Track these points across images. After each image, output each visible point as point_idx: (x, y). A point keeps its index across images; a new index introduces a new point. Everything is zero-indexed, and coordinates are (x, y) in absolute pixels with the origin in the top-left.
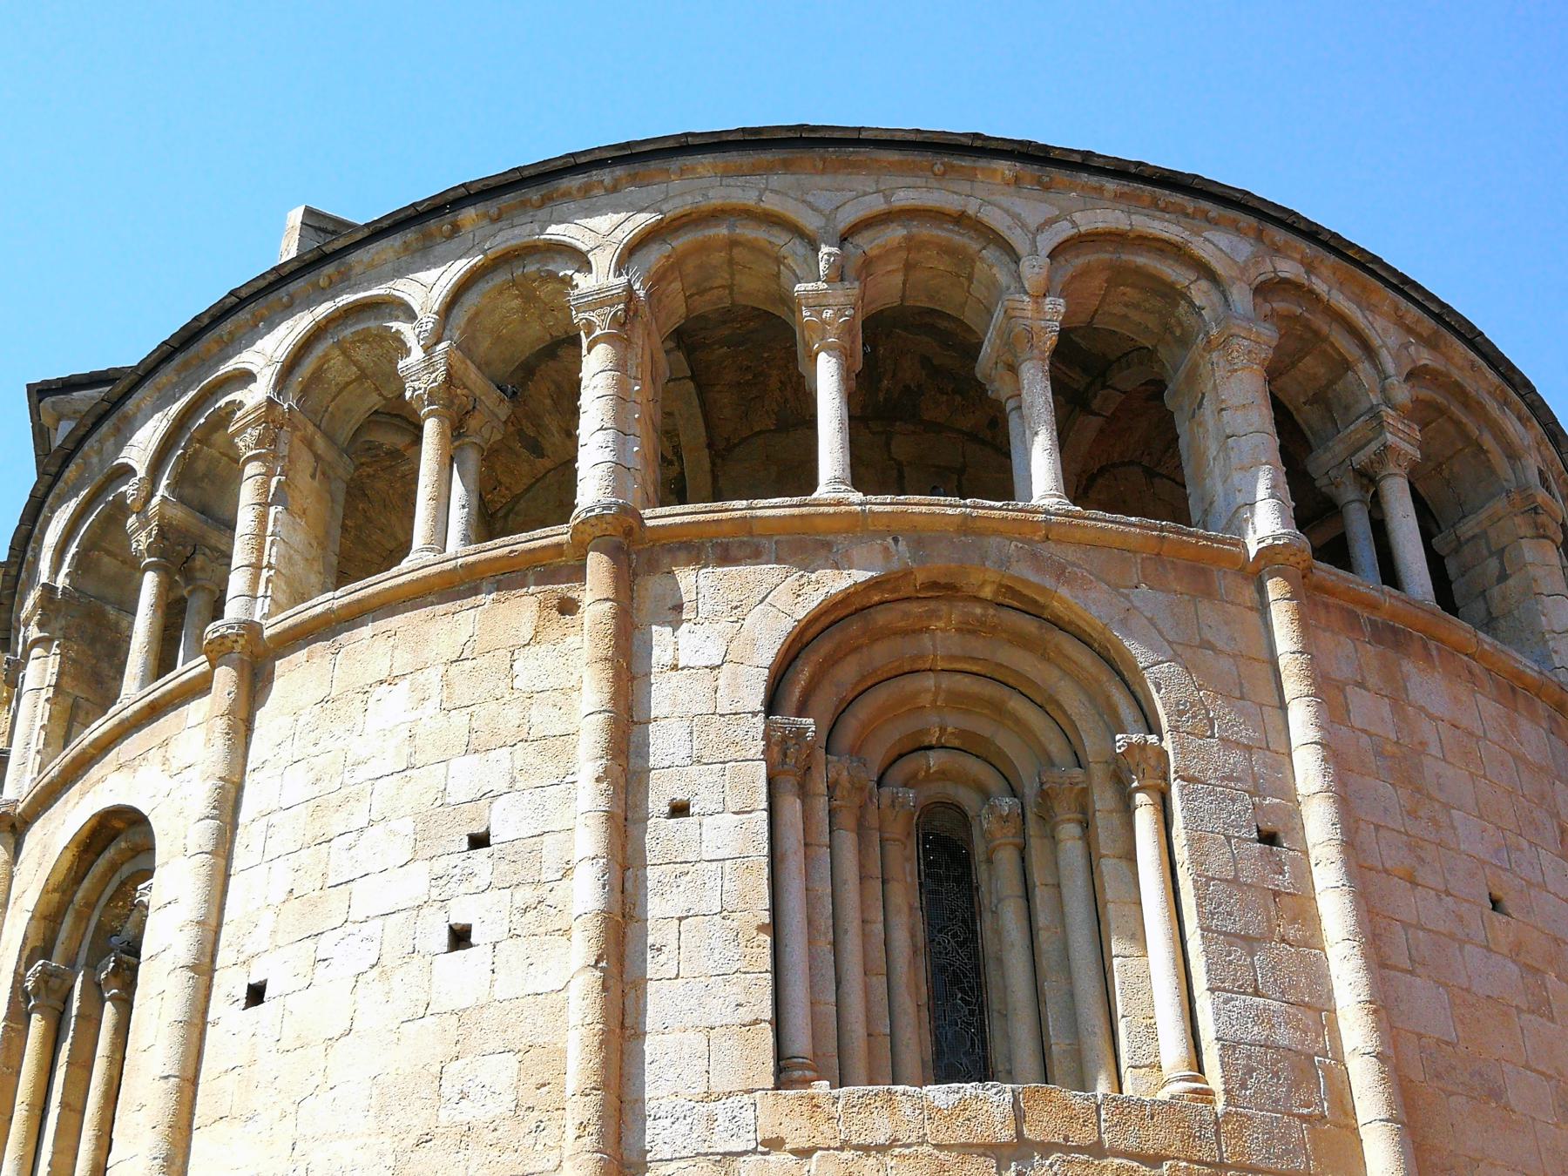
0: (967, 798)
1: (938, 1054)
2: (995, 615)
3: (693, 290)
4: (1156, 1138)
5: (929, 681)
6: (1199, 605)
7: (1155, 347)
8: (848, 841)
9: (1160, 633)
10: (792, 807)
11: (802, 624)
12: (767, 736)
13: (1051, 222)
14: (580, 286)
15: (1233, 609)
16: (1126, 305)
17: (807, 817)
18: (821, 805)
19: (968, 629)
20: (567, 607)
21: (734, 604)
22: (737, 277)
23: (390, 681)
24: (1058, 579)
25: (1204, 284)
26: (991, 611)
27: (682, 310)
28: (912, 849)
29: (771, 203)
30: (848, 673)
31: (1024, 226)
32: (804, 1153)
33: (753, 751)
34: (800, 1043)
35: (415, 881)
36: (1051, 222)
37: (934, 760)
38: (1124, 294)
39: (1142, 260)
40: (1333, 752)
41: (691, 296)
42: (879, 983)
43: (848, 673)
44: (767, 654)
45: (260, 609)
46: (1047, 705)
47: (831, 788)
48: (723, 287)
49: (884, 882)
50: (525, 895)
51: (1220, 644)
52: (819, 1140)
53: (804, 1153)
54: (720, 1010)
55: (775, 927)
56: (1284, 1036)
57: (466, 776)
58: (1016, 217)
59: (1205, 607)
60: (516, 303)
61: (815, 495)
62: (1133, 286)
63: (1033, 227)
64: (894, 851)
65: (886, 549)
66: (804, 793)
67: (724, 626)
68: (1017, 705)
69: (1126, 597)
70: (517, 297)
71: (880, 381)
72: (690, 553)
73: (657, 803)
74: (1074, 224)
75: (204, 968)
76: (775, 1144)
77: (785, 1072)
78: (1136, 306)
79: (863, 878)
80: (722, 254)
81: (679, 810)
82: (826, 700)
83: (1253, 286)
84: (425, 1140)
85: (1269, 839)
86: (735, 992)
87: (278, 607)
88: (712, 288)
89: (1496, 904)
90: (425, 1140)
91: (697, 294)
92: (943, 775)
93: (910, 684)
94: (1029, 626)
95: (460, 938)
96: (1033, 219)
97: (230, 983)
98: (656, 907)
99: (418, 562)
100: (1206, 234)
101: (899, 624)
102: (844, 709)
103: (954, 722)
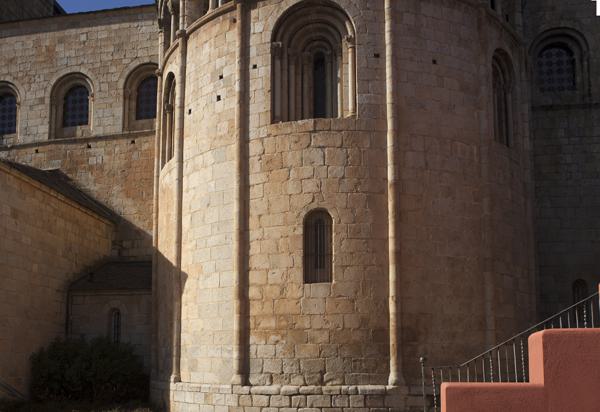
0: (324, 51)
1: (315, 111)
4: (342, 126)
5: (311, 26)
8: (292, 67)
10: (278, 63)
12: (271, 48)
17: (281, 65)
18: (285, 61)
19: (318, 12)
20: (235, 21)
23: (206, 42)
28: (312, 64)
30: (292, 28)
32: (275, 136)
34: (278, 113)
35: (210, 88)
37: (316, 43)
40: (393, 32)
42: (299, 98)
43: (292, 28)
44: (271, 28)
45: (186, 25)
46: (336, 28)
47: (288, 55)
49: (302, 74)
50: (229, 88)
53: (275, 136)
54: (262, 110)
55: (273, 91)
56: (373, 102)
57: (219, 62)
64: (305, 68)
66: (281, 58)
67: (263, 22)
68: (332, 30)
73: (251, 66)
75: (182, 107)
76: (269, 136)
77: (274, 120)
79: (296, 73)
81: (255, 67)
82: (287, 37)
84: (215, 139)
85: (377, 56)
86: (264, 105)
87: (189, 25)
89: (434, 62)
90: (215, 139)
92: (318, 46)
93: (308, 27)
94: (330, 10)
95: (219, 98)
97: (186, 110)
98: (252, 89)
99: (210, 12)
102: (293, 35)
103: (318, 34)
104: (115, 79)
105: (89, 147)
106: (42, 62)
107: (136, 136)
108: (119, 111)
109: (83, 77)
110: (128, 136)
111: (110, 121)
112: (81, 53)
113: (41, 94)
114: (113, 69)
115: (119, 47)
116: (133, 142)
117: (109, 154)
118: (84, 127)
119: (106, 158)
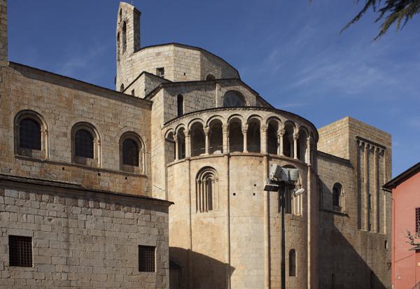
104: (114, 136)
105: (99, 174)
106: (61, 107)
107: (129, 175)
108: (117, 157)
109: (92, 127)
110: (123, 174)
111: (112, 161)
112: (92, 111)
113: (64, 130)
114: (112, 129)
115: (116, 116)
116: (126, 178)
117: (113, 182)
118: (91, 159)
119: (111, 184)
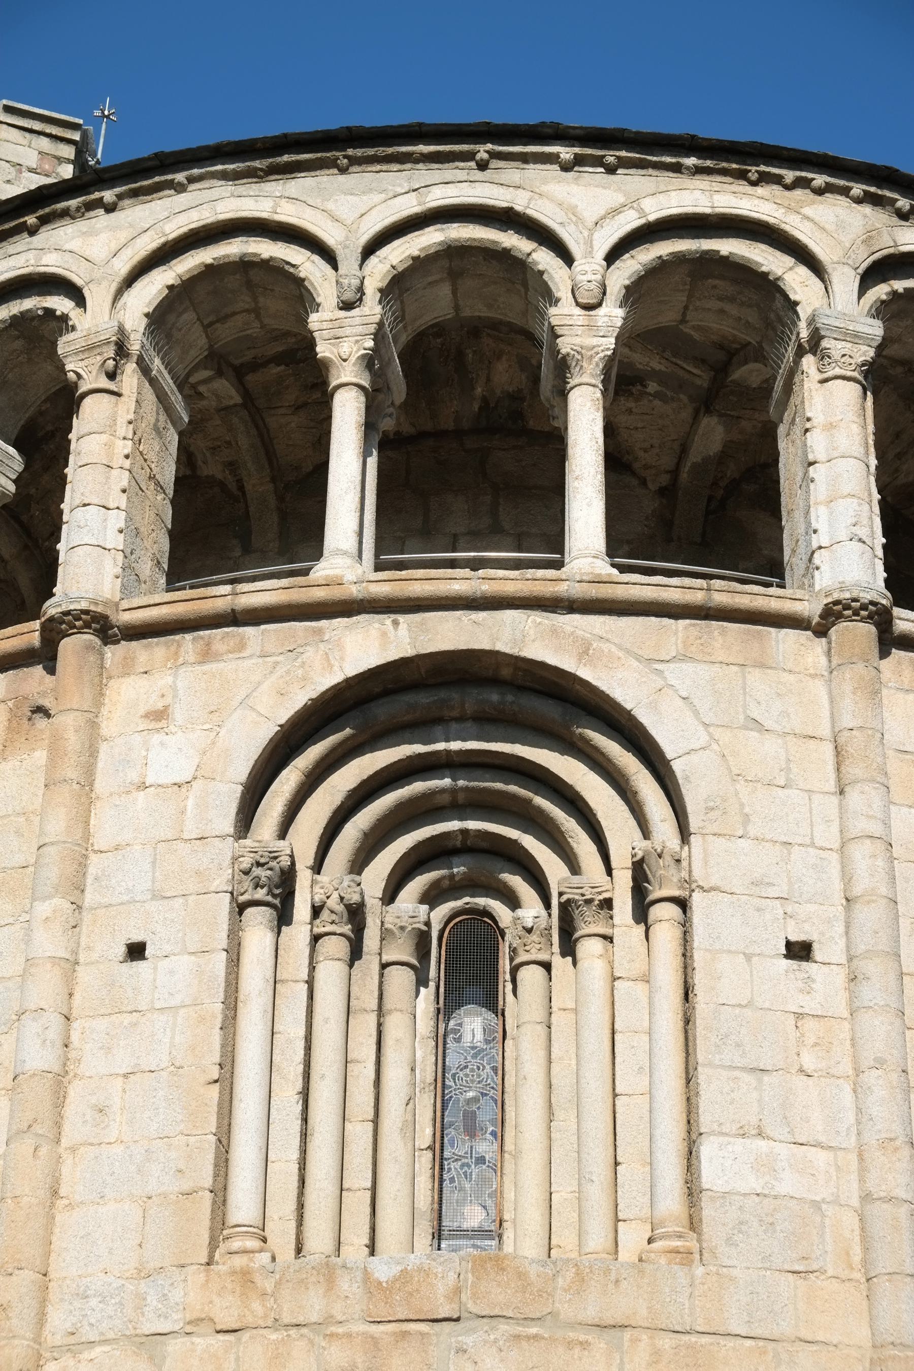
2: (513, 702)
3: (212, 318)
6: (748, 676)
7: (760, 343)
9: (696, 713)
11: (286, 728)
13: (615, 211)
14: (79, 327)
15: (792, 678)
16: (720, 299)
21: (213, 708)
22: (261, 300)
24: (580, 660)
25: (803, 271)
26: (510, 698)
27: (203, 342)
29: (287, 214)
31: (579, 220)
33: (217, 882)
36: (615, 211)
38: (715, 287)
39: (727, 246)
41: (211, 324)
48: (247, 311)
51: (768, 724)
52: (250, 1320)
58: (572, 210)
59: (755, 677)
60: (19, 344)
61: (322, 570)
62: (722, 277)
63: (590, 223)
65: (384, 634)
69: (660, 672)
70: (18, 337)
71: (473, 389)
72: (168, 647)
74: (642, 213)
78: (732, 300)
80: (238, 276)
83: (860, 271)
88: (234, 314)
91: (217, 321)
96: (590, 214)
100: (807, 211)
101: (405, 718)
